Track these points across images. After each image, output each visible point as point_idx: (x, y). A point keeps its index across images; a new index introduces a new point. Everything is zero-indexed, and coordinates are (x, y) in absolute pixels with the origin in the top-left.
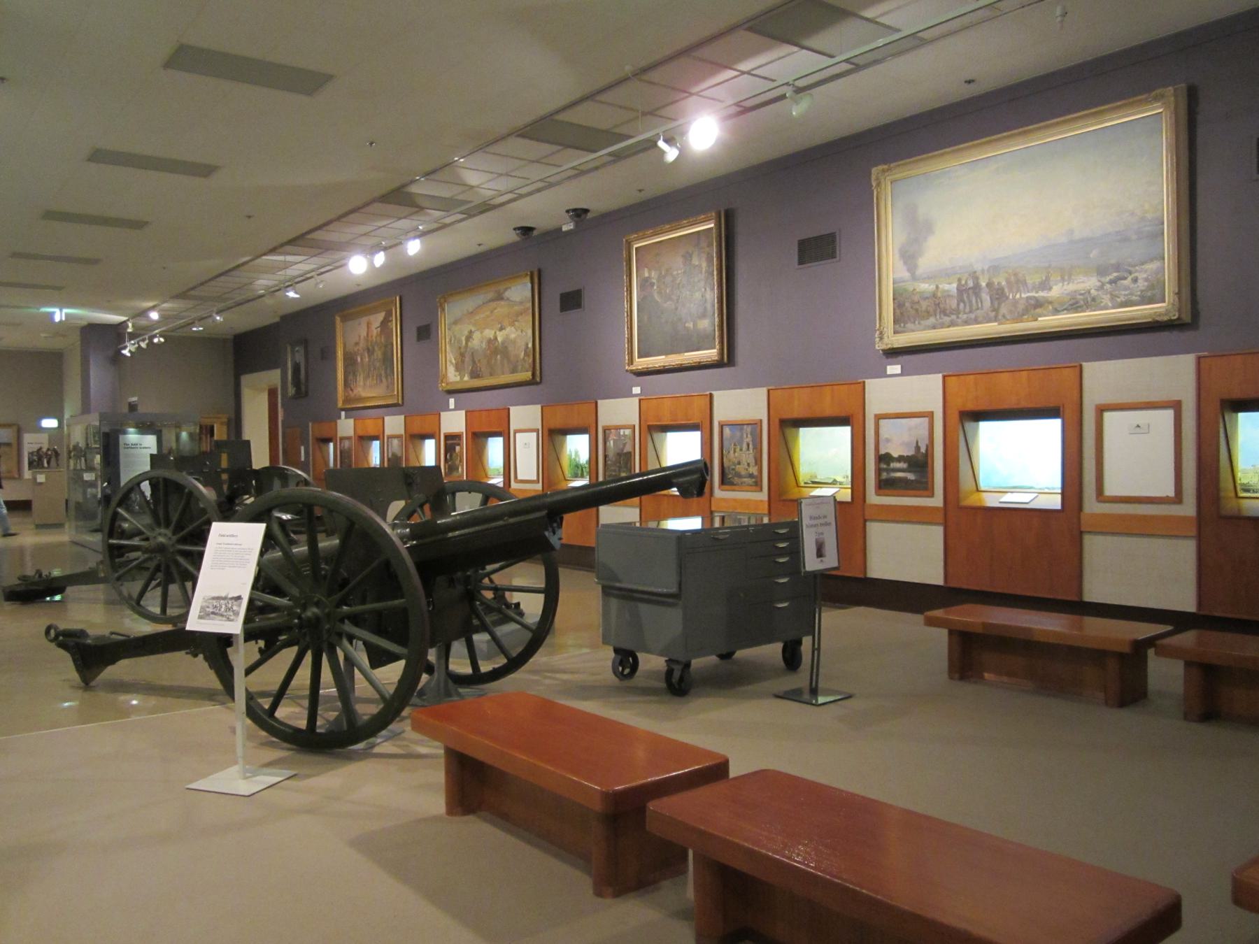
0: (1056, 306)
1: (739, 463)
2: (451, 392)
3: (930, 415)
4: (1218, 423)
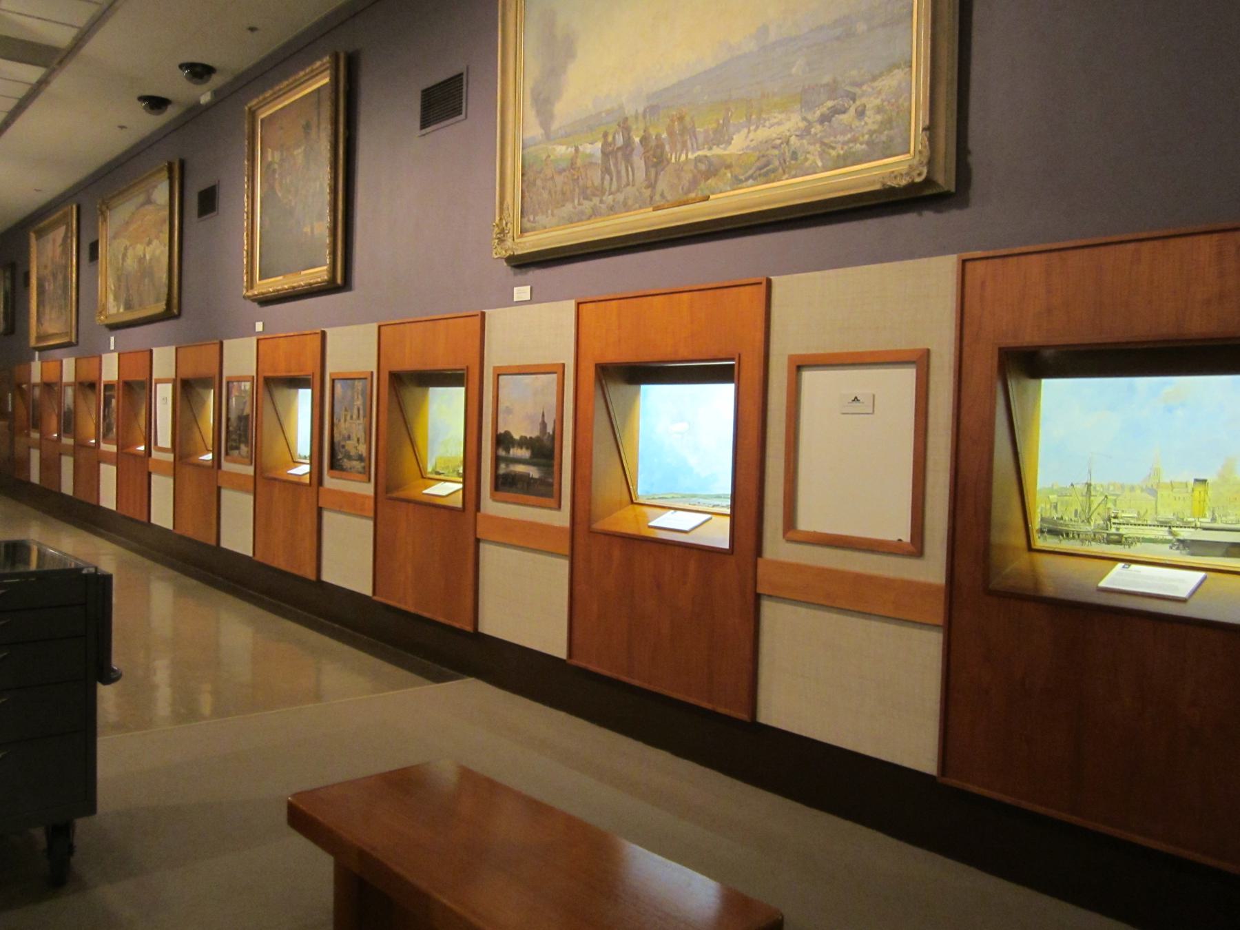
0: (737, 171)
1: (349, 438)
2: (114, 327)
4: (993, 398)
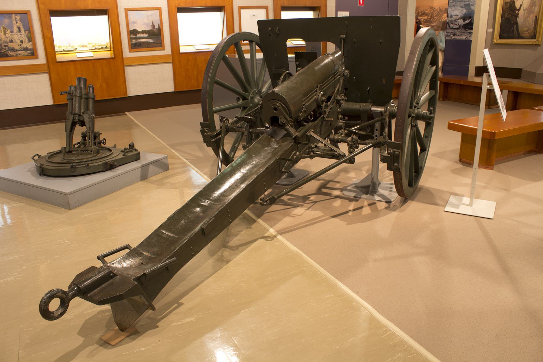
1: (11, 41)
3: (159, 9)
